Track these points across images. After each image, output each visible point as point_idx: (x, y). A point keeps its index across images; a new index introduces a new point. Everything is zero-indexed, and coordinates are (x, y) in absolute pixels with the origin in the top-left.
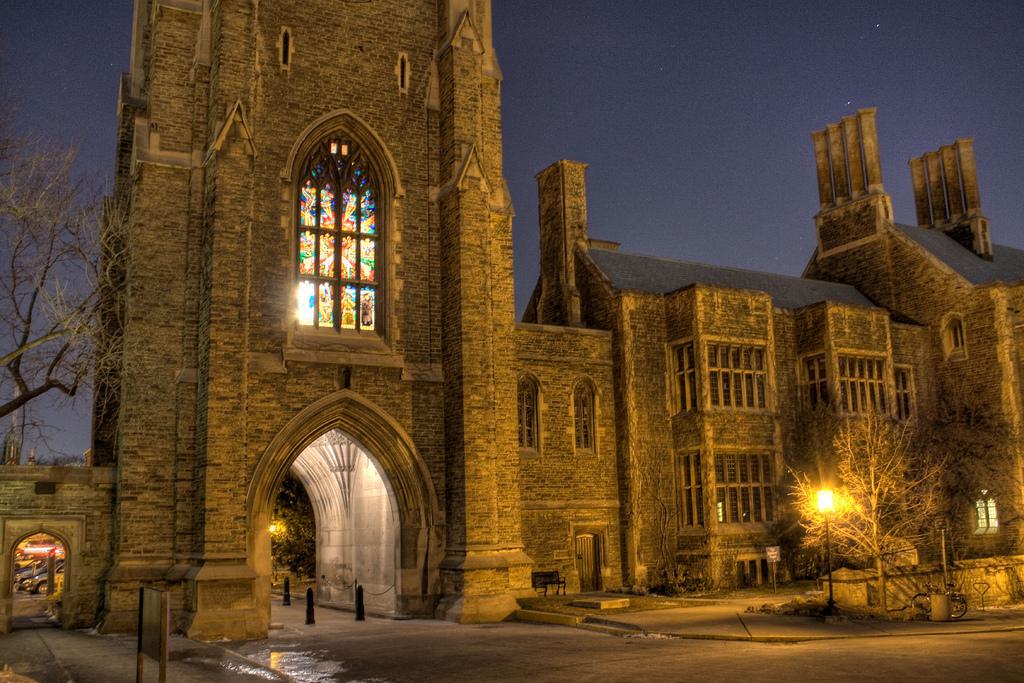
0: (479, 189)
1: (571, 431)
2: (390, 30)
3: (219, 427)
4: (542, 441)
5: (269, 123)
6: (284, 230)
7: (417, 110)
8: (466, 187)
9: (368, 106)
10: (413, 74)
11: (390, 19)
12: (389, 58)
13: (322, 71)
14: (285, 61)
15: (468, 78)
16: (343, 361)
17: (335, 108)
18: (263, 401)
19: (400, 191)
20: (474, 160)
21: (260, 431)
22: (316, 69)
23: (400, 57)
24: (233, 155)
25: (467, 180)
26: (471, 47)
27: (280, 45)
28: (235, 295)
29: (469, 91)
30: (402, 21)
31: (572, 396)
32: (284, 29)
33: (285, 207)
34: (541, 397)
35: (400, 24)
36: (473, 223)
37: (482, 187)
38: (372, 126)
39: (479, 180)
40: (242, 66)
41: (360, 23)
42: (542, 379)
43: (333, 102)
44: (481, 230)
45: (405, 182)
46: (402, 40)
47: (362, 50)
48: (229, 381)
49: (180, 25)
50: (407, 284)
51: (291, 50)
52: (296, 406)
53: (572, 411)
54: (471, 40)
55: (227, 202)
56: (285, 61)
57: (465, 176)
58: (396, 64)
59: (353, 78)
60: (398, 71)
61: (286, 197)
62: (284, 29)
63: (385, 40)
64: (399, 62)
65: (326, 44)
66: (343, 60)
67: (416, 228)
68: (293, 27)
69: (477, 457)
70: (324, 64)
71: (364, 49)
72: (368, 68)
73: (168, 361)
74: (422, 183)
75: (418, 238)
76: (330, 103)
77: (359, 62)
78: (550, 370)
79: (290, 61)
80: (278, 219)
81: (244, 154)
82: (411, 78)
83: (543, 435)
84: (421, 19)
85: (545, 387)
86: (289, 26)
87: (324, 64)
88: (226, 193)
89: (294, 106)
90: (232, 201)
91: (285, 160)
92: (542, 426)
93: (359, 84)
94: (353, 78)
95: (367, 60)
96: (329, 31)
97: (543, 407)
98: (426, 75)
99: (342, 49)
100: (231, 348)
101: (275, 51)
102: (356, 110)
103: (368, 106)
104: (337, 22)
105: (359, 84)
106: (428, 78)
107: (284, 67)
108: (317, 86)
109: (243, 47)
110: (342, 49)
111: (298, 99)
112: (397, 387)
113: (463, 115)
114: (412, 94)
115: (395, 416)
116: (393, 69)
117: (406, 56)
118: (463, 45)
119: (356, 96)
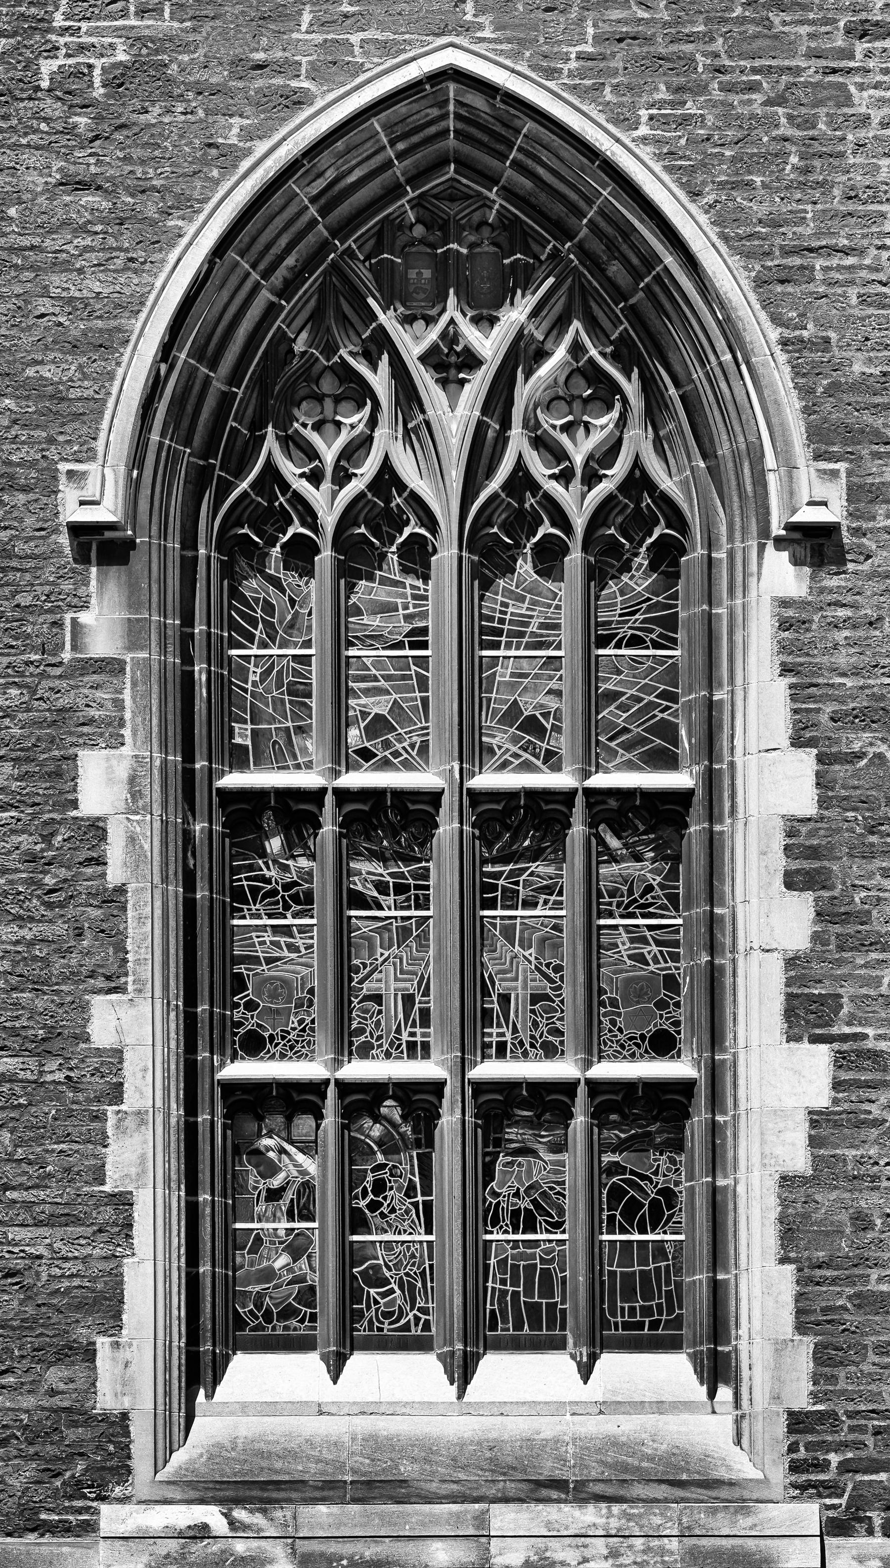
6: (96, 829)
33: (94, 699)
50: (855, 1064)
80: (63, 773)
91: (94, 408)
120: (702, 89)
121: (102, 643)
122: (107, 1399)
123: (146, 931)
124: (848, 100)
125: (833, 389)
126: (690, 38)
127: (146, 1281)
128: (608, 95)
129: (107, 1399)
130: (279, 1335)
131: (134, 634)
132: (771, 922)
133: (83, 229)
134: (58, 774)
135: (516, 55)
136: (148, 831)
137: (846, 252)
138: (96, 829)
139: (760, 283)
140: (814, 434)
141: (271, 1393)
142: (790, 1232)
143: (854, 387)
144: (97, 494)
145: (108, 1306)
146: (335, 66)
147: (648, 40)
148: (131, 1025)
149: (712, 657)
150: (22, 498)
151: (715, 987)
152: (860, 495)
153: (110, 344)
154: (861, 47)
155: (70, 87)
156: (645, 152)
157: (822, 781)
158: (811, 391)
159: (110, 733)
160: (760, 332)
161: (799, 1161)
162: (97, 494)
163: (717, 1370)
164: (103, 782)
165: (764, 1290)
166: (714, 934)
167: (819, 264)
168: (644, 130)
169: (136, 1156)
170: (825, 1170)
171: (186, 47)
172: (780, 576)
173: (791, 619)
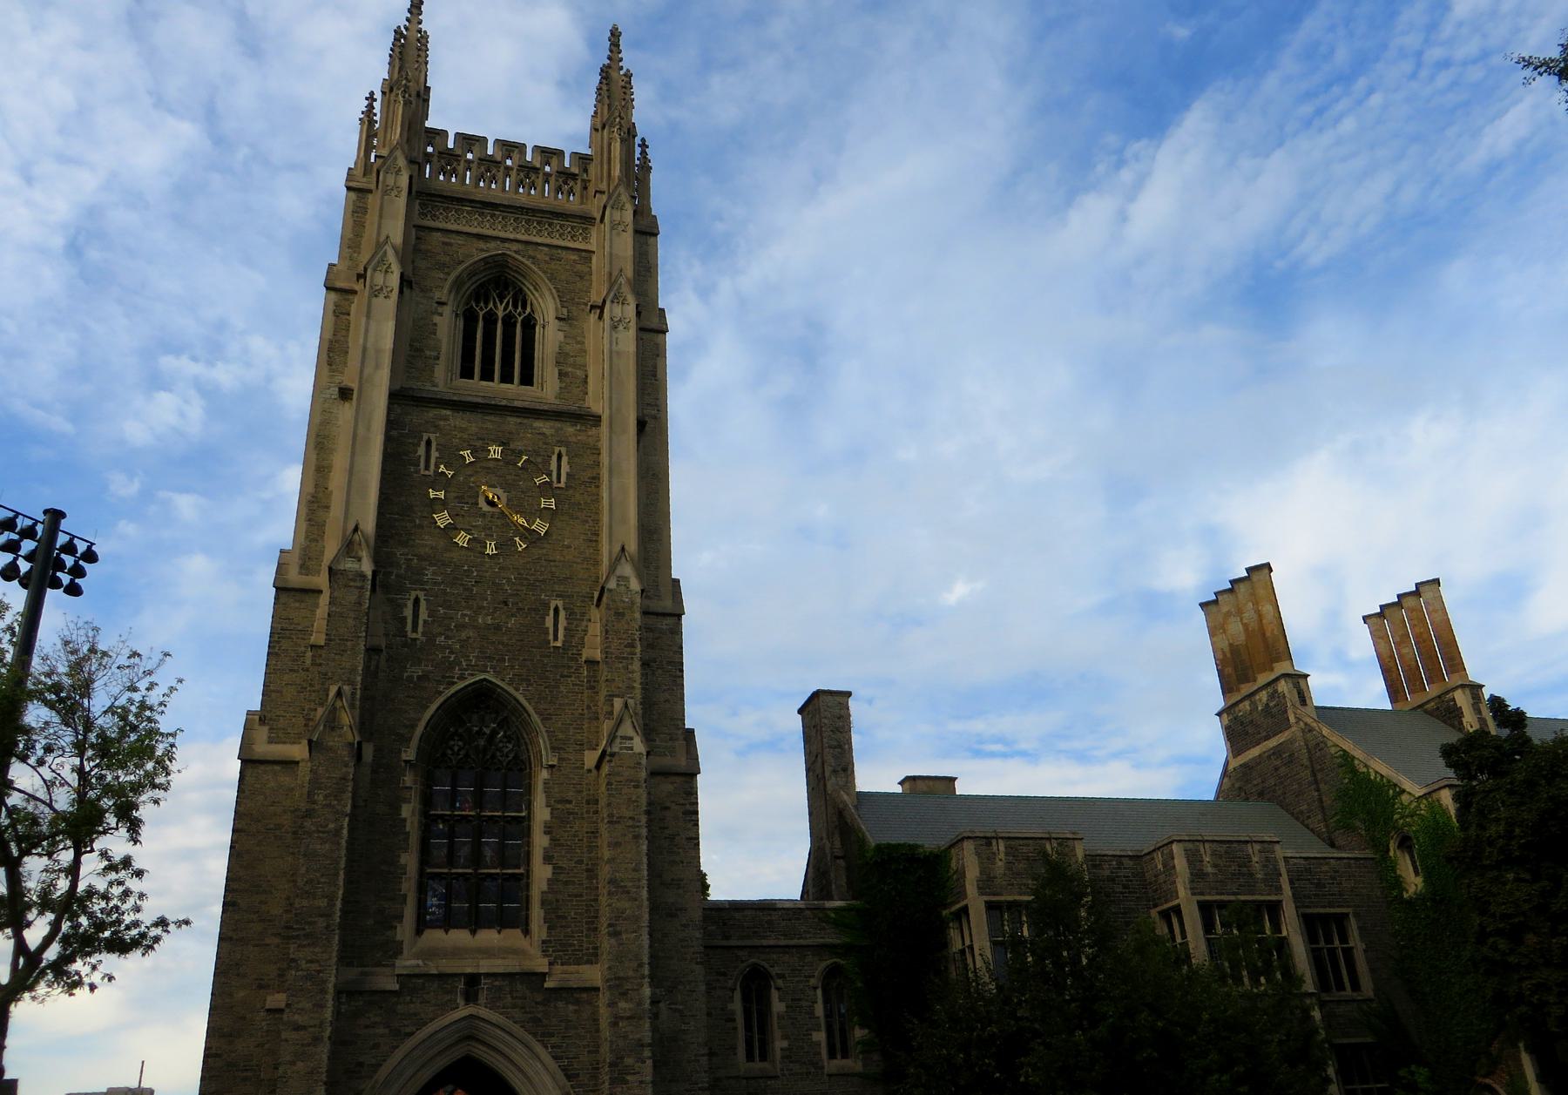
1: (820, 1036)
3: (293, 1063)
4: (778, 1054)
6: (405, 820)
7: (572, 664)
16: (469, 970)
18: (367, 1027)
21: (361, 1064)
27: (408, 612)
28: (323, 903)
31: (819, 992)
34: (775, 995)
42: (774, 971)
46: (556, 587)
48: (308, 1006)
52: (408, 1030)
53: (819, 1010)
56: (415, 629)
60: (549, 622)
67: (570, 802)
69: (627, 1082)
73: (260, 987)
78: (786, 958)
79: (420, 629)
80: (398, 809)
83: (779, 1044)
85: (780, 982)
90: (326, 797)
92: (777, 1033)
97: (778, 1006)
100: (315, 966)
112: (539, 998)
114: (566, 647)
115: (535, 1035)
117: (560, 603)
122: (399, 938)
123: (414, 840)
127: (409, 912)
129: (399, 938)
130: (433, 925)
131: (415, 782)
132: (540, 841)
136: (416, 819)
138: (405, 820)
141: (435, 937)
142: (543, 903)
144: (410, 754)
145: (400, 918)
146: (462, 678)
148: (410, 860)
149: (529, 790)
151: (528, 854)
153: (413, 727)
155: (410, 679)
161: (545, 888)
163: (526, 932)
164: (407, 811)
165: (537, 914)
166: (529, 844)
169: (409, 886)
170: (551, 890)
172: (545, 774)
173: (546, 783)
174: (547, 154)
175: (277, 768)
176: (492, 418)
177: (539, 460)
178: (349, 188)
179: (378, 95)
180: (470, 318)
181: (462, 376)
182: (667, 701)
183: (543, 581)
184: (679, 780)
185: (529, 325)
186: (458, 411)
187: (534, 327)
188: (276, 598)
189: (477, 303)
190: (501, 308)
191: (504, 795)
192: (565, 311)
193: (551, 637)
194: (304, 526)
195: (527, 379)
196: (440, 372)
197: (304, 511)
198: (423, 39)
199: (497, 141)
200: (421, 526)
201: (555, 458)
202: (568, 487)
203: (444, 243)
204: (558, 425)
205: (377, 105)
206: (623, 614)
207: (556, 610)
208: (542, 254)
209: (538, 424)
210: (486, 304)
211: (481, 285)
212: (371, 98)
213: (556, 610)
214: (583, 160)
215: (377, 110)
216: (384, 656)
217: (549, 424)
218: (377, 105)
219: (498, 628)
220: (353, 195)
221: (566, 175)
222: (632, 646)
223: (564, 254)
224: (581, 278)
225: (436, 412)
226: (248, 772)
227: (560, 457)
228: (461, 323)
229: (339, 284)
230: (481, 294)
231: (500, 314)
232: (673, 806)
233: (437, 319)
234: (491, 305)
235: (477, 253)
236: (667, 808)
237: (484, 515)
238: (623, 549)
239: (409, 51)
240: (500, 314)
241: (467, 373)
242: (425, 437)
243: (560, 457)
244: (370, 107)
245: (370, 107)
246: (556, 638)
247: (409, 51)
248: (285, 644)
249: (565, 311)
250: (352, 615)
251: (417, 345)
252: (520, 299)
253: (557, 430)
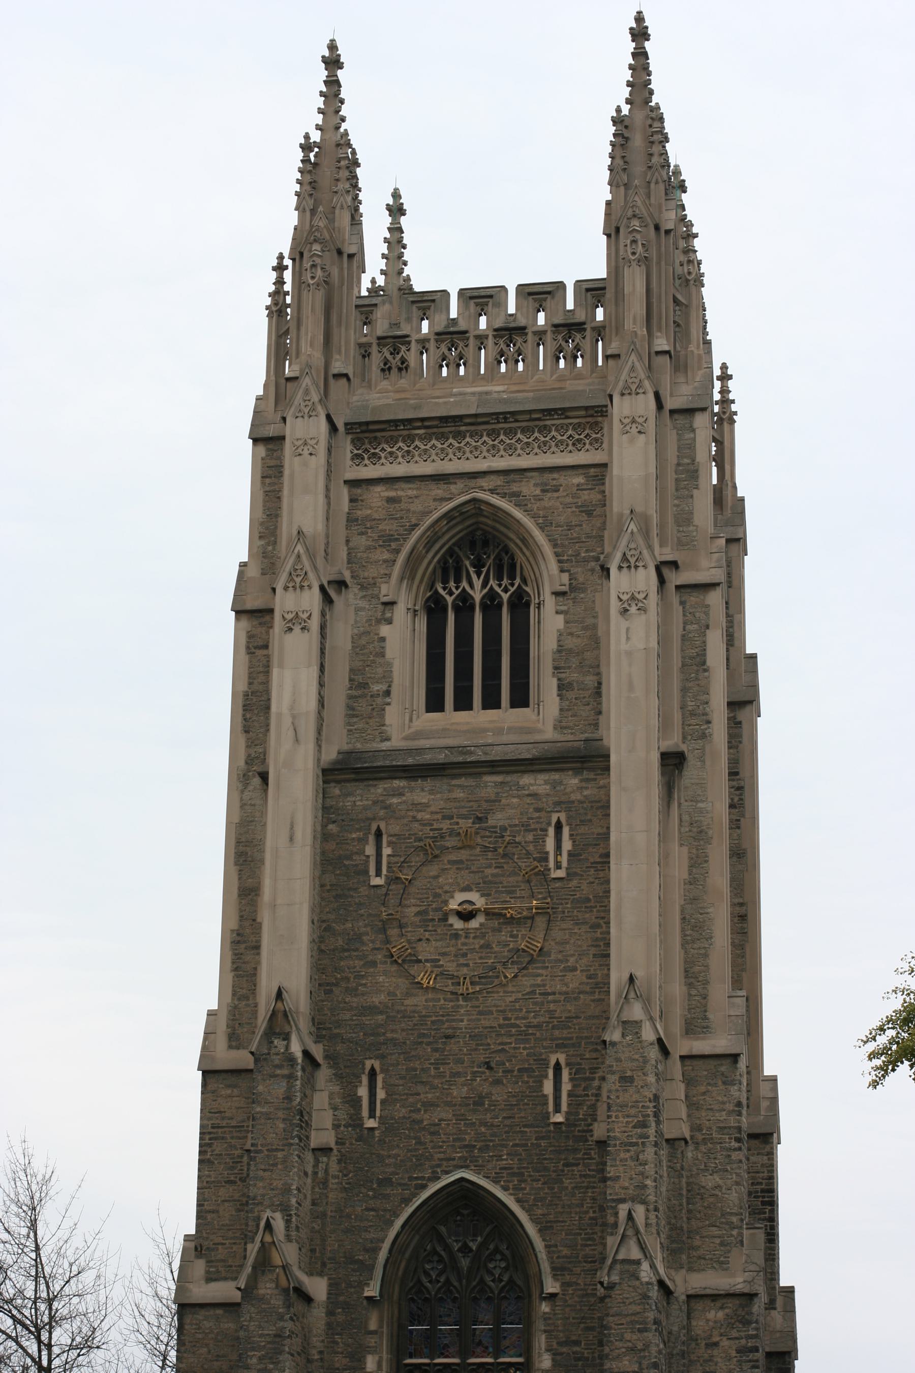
0: (638, 1279)
2: (535, 1021)
5: (348, 1216)
8: (615, 1278)
9: (499, 1158)
10: (574, 1086)
11: (535, 1004)
12: (534, 1070)
13: (426, 1118)
14: (372, 1115)
15: (632, 1090)
17: (447, 1173)
19: (551, 1286)
20: (630, 1232)
22: (415, 1116)
23: (553, 1062)
24: (261, 1292)
25: (618, 1266)
26: (637, 1035)
27: (363, 1092)
29: (633, 1111)
30: (554, 1001)
32: (368, 1064)
33: (372, 1341)
35: (552, 1006)
36: (628, 1336)
37: (643, 1274)
38: (505, 1189)
39: (638, 1263)
40: (280, 1155)
41: (487, 1023)
43: (445, 1163)
44: (640, 1346)
45: (557, 1271)
46: (557, 1033)
47: (490, 1068)
49: (229, 1092)
51: (381, 1094)
54: (638, 1024)
55: (254, 1360)
57: (615, 1261)
58: (546, 1077)
59: (473, 1118)
60: (548, 1087)
61: (373, 1326)
62: (368, 1064)
63: (527, 1041)
64: (551, 1073)
65: (433, 1072)
66: (459, 1092)
67: (577, 1343)
68: (382, 1057)
70: (429, 1105)
71: (493, 1065)
72: (499, 1094)
74: (588, 1266)
75: (579, 1359)
76: (439, 1166)
77: (486, 1088)
79: (378, 1113)
80: (362, 1361)
81: (277, 1287)
82: (570, 1095)
84: (588, 988)
86: (377, 1058)
87: (429, 1105)
88: (253, 1349)
89: (386, 1182)
91: (372, 1268)
93: (485, 1124)
94: (473, 1118)
95: (498, 1082)
96: (436, 1050)
98: (596, 1083)
99: (458, 1074)
101: (355, 1102)
102: (478, 1171)
103: (499, 1158)
104: (450, 1032)
105: (485, 1124)
106: (599, 1088)
107: (371, 1123)
108: (419, 1142)
109: (281, 1126)
110: (458, 1074)
111: (391, 1170)
113: (622, 1155)
114: (570, 1122)
116: (541, 1085)
118: (623, 1035)
119: (479, 1145)
120: (525, 1181)
121: (373, 1326)
124: (563, 1183)
125: (558, 1257)
126: (524, 1168)
128: (502, 1183)
133: (371, 1221)
134: (360, 1361)
135: (479, 1174)
137: (562, 1222)
139: (540, 1231)
140: (553, 1269)
143: (563, 1257)
144: (372, 1290)
147: (512, 1168)
150: (353, 1290)
152: (565, 1285)
153: (376, 1250)
154: (566, 1169)
156: (512, 1197)
157: (553, 1360)
158: (552, 1258)
159: (374, 1351)
160: (539, 1244)
162: (372, 1290)
167: (555, 1225)
168: (511, 1191)
171: (397, 1174)
174: (539, 294)
175: (219, 1312)
176: (462, 781)
177: (530, 837)
178: (256, 441)
179: (287, 262)
180: (434, 610)
181: (429, 710)
182: (718, 1187)
183: (538, 1026)
184: (731, 1304)
185: (521, 605)
186: (414, 778)
187: (528, 605)
188: (204, 1085)
189: (445, 581)
190: (478, 583)
191: (497, 1334)
192: (565, 577)
193: (551, 1108)
194: (230, 976)
195: (520, 699)
196: (393, 716)
197: (229, 955)
198: (344, 142)
199: (462, 292)
200: (374, 964)
201: (551, 831)
202: (570, 875)
203: (390, 500)
204: (556, 776)
205: (288, 275)
206: (631, 1080)
207: (558, 1068)
208: (528, 488)
209: (526, 780)
210: (458, 581)
211: (451, 552)
212: (280, 268)
213: (558, 1068)
214: (592, 291)
215: (288, 287)
216: (334, 1159)
217: (542, 777)
218: (288, 275)
219: (479, 1101)
220: (262, 450)
221: (570, 329)
222: (644, 1125)
223: (562, 479)
224: (589, 514)
225: (387, 784)
226: (187, 1320)
227: (559, 827)
228: (422, 625)
229: (249, 606)
230: (450, 569)
231: (477, 595)
232: (725, 1343)
233: (385, 630)
234: (464, 584)
235: (435, 506)
236: (716, 1344)
237: (456, 936)
238: (631, 979)
239: (328, 172)
240: (477, 595)
241: (435, 703)
242: (374, 828)
243: (559, 827)
244: (280, 282)
245: (280, 282)
246: (557, 1110)
247: (328, 172)
248: (218, 1147)
249: (565, 577)
250: (280, 1114)
251: (360, 678)
252: (507, 566)
253: (554, 784)
